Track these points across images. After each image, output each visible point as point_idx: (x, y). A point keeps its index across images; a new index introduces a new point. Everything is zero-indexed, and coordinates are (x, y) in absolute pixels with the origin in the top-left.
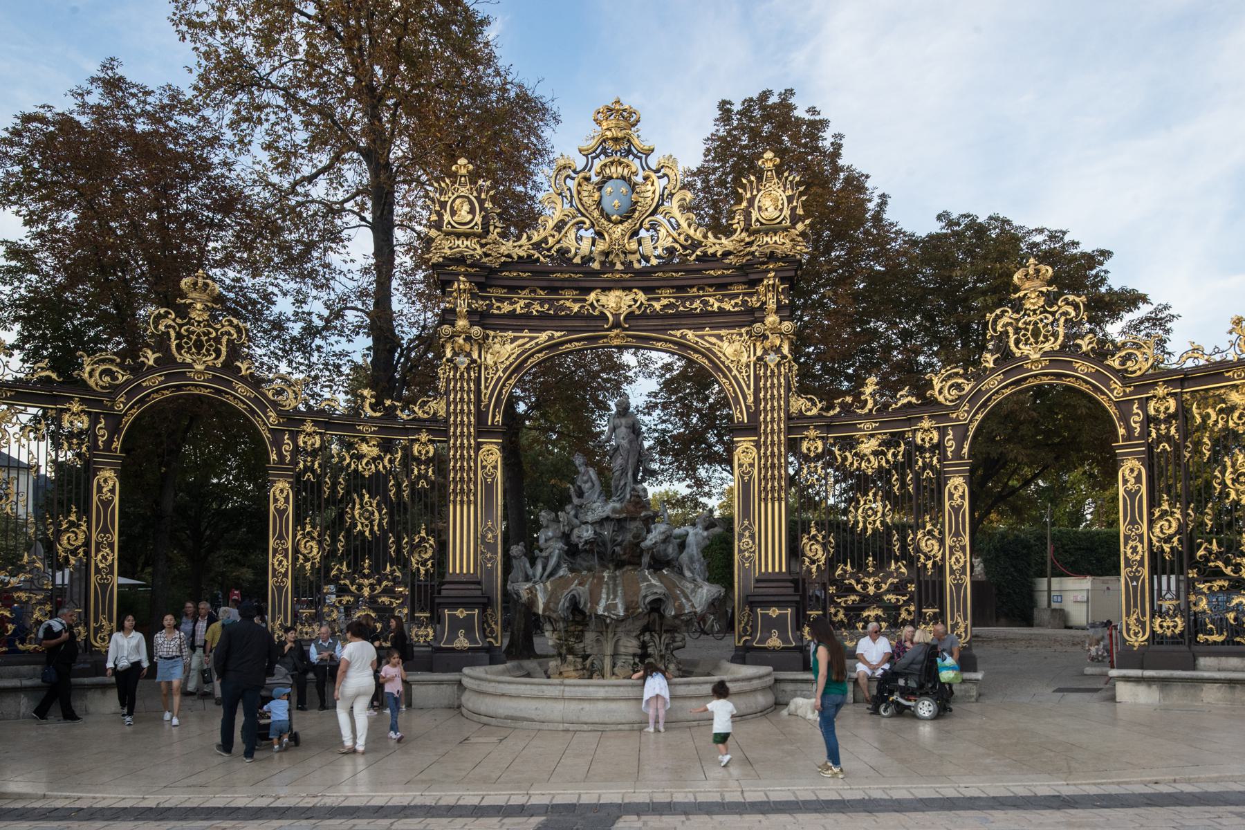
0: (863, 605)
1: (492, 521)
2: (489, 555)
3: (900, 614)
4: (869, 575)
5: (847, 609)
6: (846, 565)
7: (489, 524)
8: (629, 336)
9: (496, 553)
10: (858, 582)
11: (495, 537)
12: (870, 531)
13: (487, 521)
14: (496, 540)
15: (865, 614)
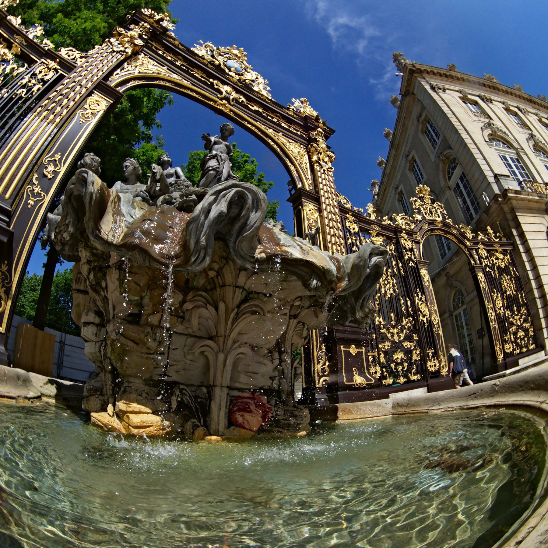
0: (394, 349)
1: (62, 156)
2: (37, 190)
3: (412, 356)
4: (394, 327)
5: (386, 353)
6: (380, 318)
7: (57, 157)
8: (231, 110)
9: (47, 193)
10: (388, 329)
11: (56, 173)
12: (389, 296)
13: (56, 152)
14: (54, 178)
15: (395, 357)
